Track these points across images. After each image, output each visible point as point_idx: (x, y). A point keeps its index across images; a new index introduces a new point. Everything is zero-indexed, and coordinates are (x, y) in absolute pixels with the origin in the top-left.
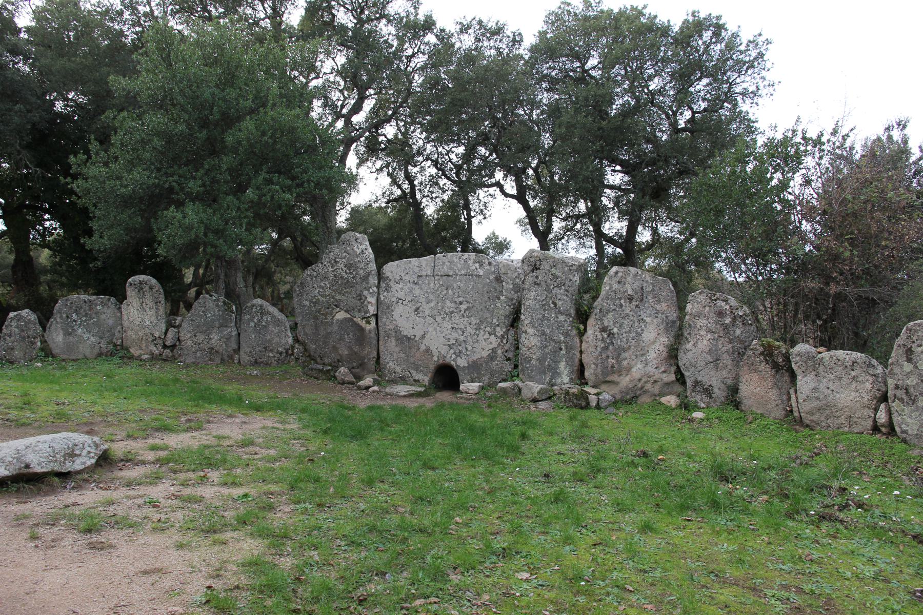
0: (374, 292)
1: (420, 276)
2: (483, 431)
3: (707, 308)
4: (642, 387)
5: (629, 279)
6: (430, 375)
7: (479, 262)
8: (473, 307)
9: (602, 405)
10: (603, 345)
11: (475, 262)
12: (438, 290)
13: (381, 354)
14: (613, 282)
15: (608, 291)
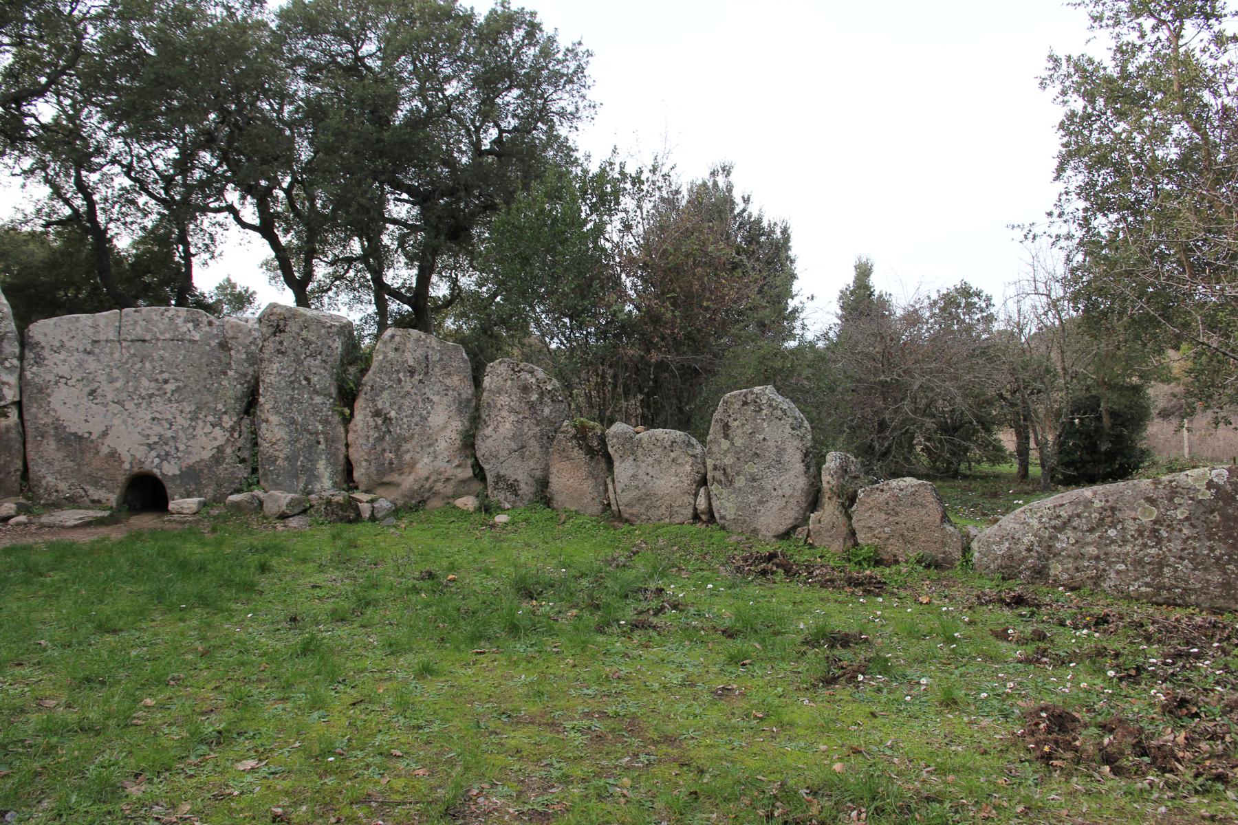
0: (13, 366)
1: (95, 342)
2: (202, 568)
3: (509, 382)
4: (431, 488)
5: (409, 345)
6: (118, 491)
7: (193, 321)
8: (185, 386)
9: (379, 515)
10: (376, 435)
11: (186, 321)
12: (127, 362)
13: (31, 464)
14: (388, 349)
15: (381, 362)
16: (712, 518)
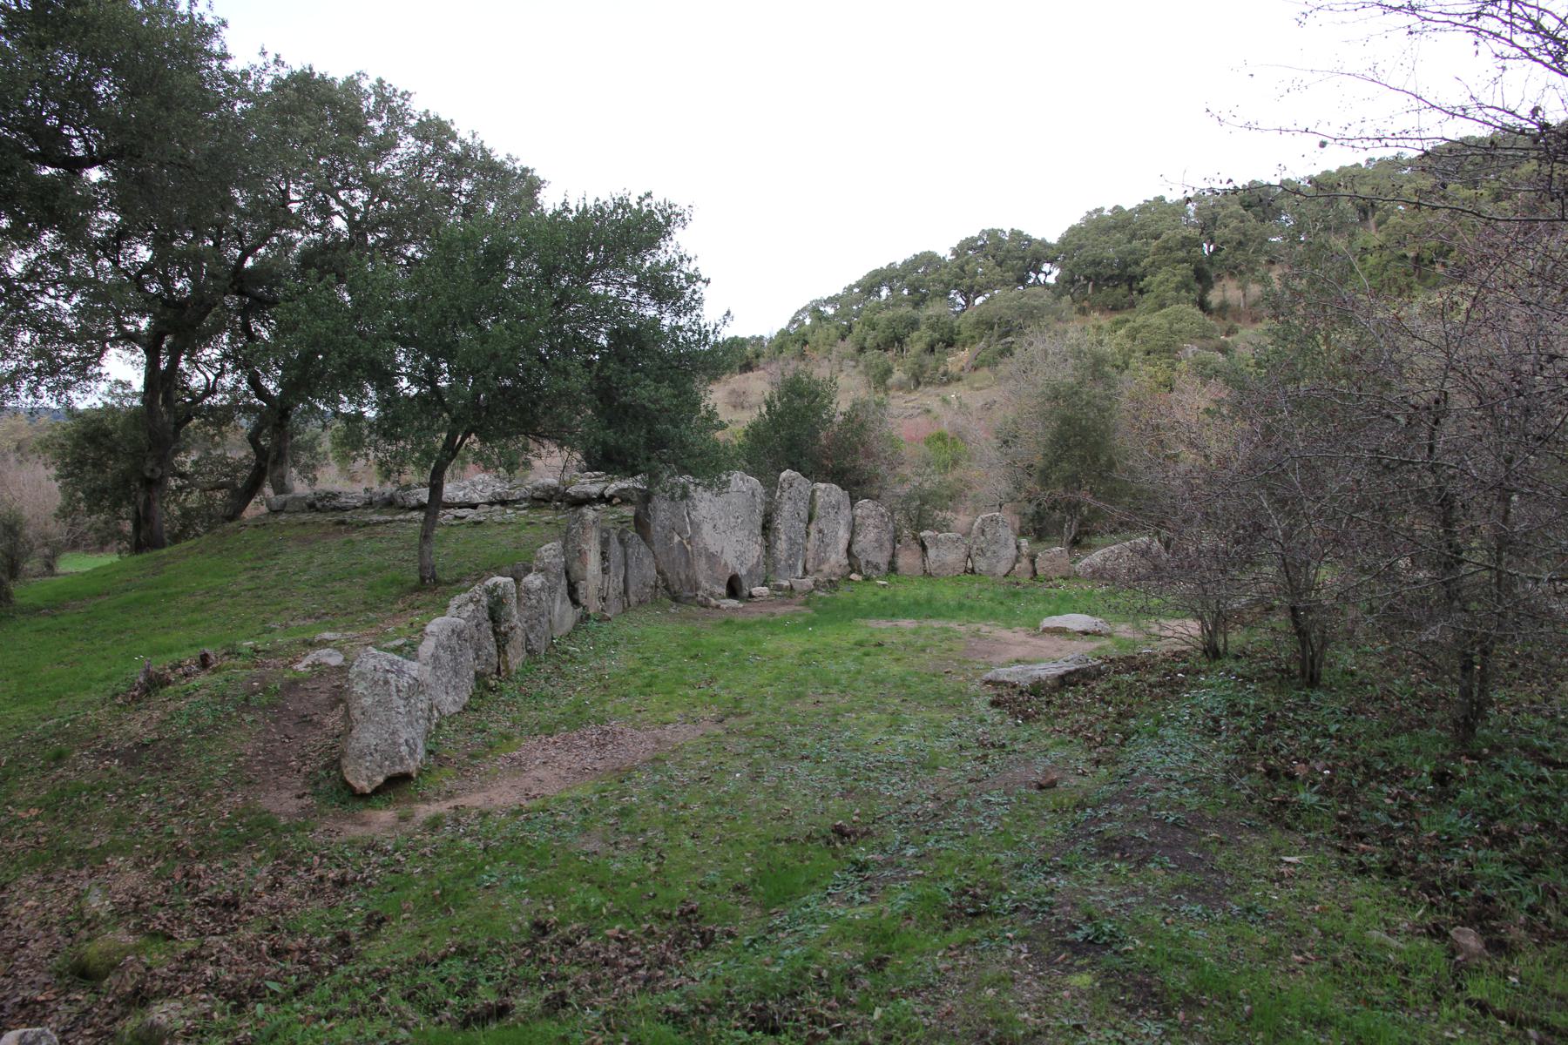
16: (973, 571)
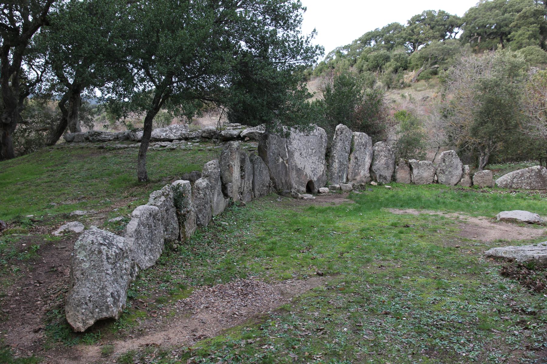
3: (385, 148)
5: (363, 138)
